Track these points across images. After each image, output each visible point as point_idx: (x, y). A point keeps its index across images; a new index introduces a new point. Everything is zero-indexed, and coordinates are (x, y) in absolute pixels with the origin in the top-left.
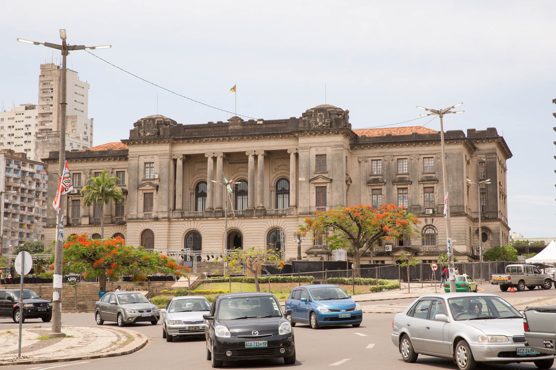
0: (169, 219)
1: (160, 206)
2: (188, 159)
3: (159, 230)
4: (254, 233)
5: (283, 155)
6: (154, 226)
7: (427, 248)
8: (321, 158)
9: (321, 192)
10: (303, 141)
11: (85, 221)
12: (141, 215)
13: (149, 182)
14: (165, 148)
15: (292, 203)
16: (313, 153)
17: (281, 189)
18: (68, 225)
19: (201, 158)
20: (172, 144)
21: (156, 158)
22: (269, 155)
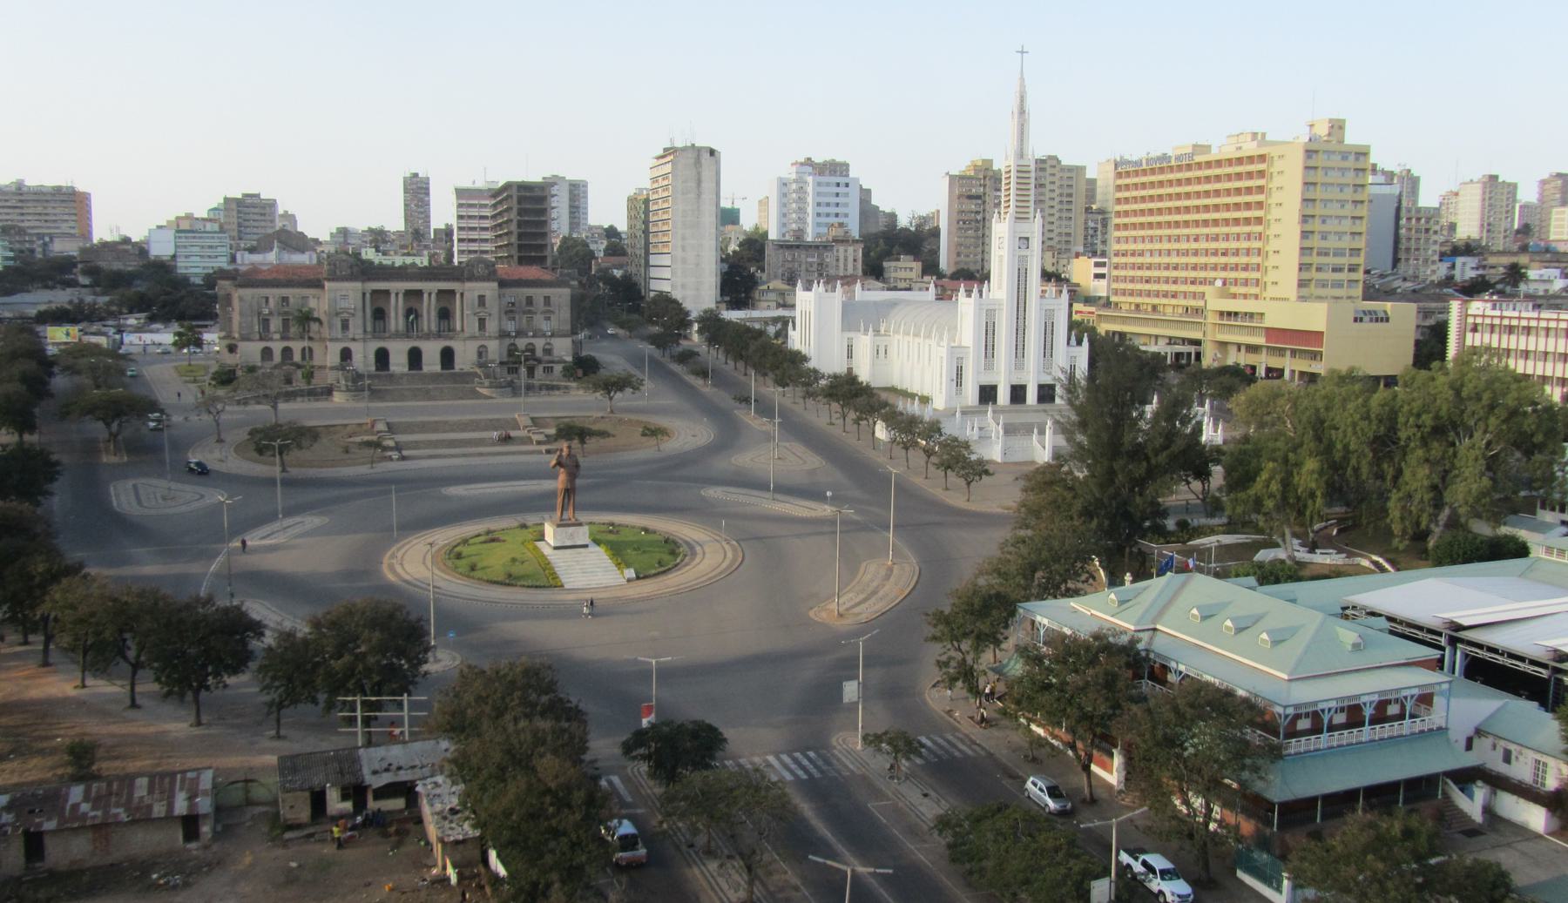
0: (364, 340)
1: (356, 328)
2: (374, 292)
3: (357, 349)
4: (431, 351)
5: (452, 292)
6: (353, 346)
7: (547, 358)
8: (482, 299)
9: (482, 322)
10: (468, 285)
11: (277, 336)
12: (340, 336)
13: (345, 310)
14: (358, 285)
15: (458, 328)
16: (476, 294)
17: (445, 315)
18: (261, 339)
19: (387, 293)
20: (363, 281)
21: (349, 294)
22: (440, 292)
